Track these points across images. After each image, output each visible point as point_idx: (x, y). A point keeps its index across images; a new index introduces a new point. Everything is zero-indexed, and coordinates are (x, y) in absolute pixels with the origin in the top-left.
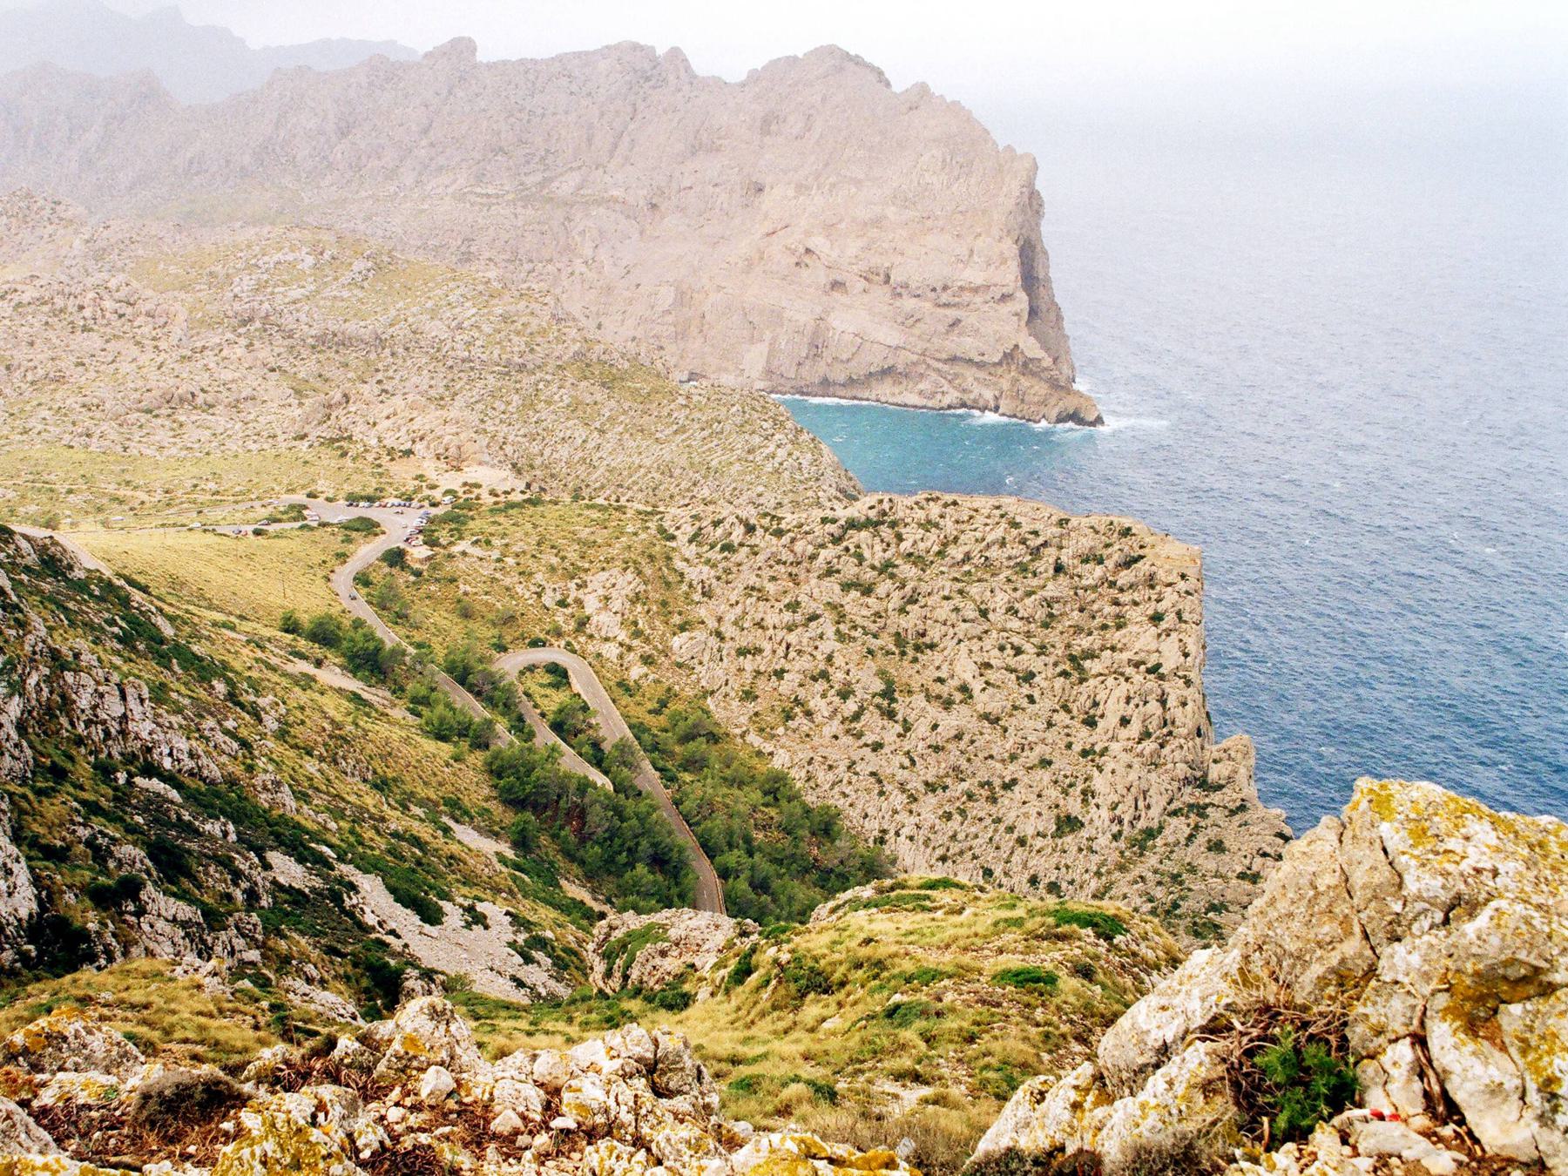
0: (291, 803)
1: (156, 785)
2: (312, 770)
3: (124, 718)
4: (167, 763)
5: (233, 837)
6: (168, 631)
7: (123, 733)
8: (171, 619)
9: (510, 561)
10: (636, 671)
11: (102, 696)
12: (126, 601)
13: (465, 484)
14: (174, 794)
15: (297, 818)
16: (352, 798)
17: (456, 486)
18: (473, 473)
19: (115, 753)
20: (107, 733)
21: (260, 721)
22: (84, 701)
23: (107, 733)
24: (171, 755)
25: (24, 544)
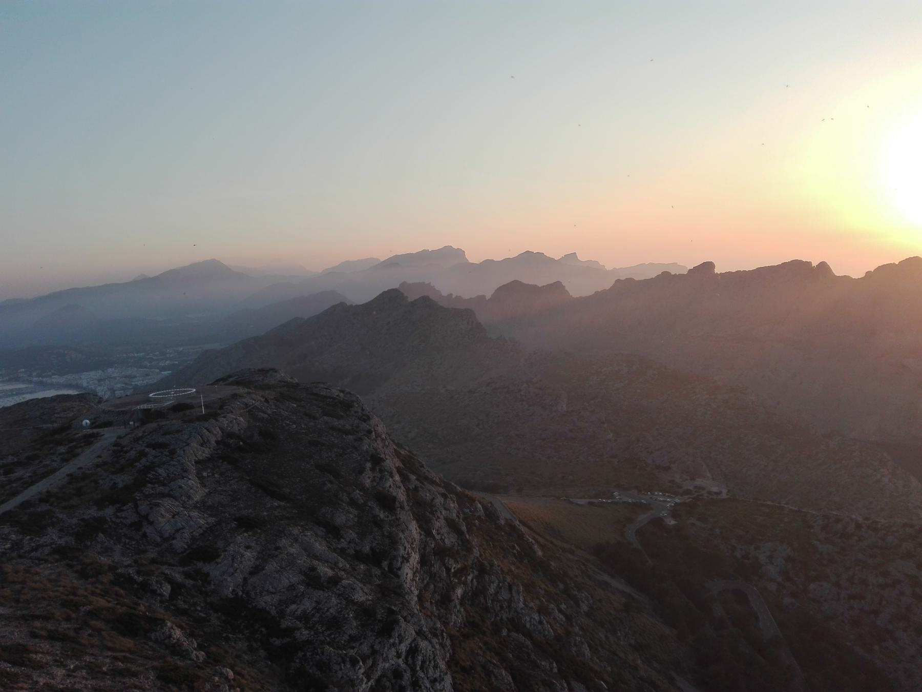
0: (587, 652)
1: (522, 638)
2: (602, 636)
3: (510, 601)
4: (528, 626)
5: (555, 670)
6: (540, 553)
7: (509, 607)
8: (543, 547)
9: (717, 531)
10: (787, 601)
11: (501, 588)
12: (521, 536)
13: (696, 487)
14: (528, 643)
15: (592, 664)
16: (622, 655)
17: (691, 488)
18: (699, 482)
19: (504, 617)
20: (502, 607)
21: (579, 606)
22: (492, 589)
23: (502, 607)
24: (530, 621)
25: (479, 506)
